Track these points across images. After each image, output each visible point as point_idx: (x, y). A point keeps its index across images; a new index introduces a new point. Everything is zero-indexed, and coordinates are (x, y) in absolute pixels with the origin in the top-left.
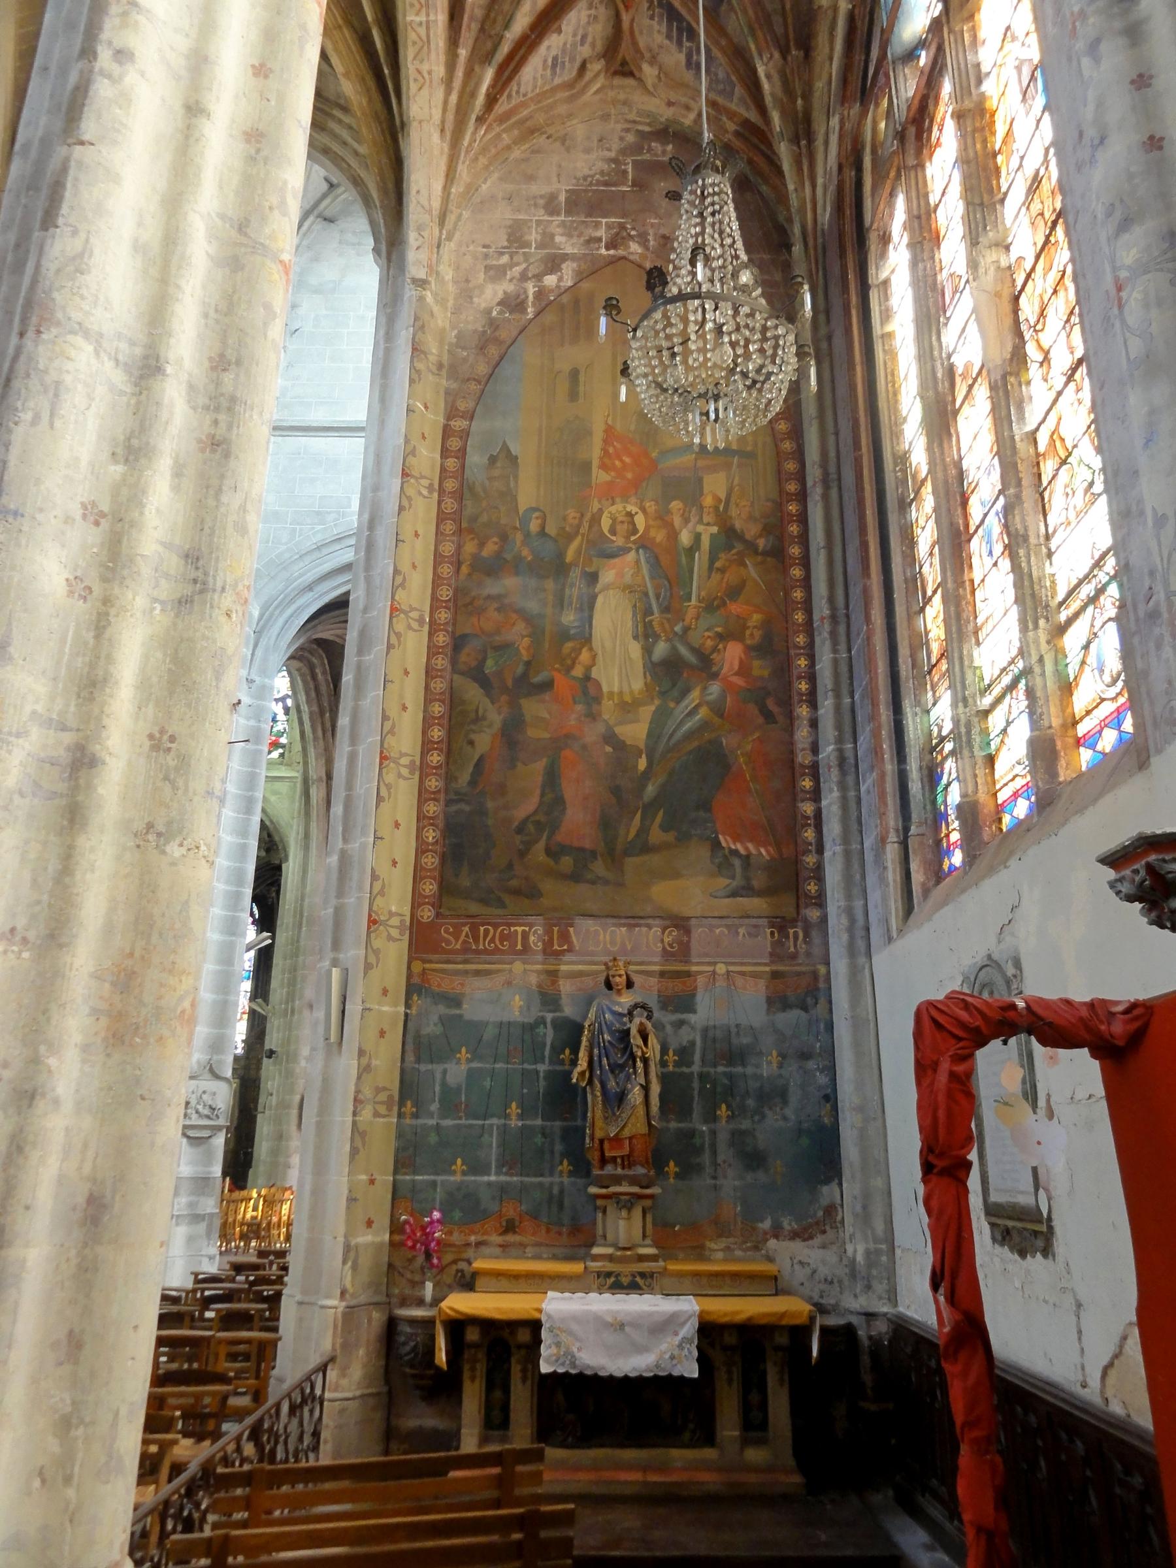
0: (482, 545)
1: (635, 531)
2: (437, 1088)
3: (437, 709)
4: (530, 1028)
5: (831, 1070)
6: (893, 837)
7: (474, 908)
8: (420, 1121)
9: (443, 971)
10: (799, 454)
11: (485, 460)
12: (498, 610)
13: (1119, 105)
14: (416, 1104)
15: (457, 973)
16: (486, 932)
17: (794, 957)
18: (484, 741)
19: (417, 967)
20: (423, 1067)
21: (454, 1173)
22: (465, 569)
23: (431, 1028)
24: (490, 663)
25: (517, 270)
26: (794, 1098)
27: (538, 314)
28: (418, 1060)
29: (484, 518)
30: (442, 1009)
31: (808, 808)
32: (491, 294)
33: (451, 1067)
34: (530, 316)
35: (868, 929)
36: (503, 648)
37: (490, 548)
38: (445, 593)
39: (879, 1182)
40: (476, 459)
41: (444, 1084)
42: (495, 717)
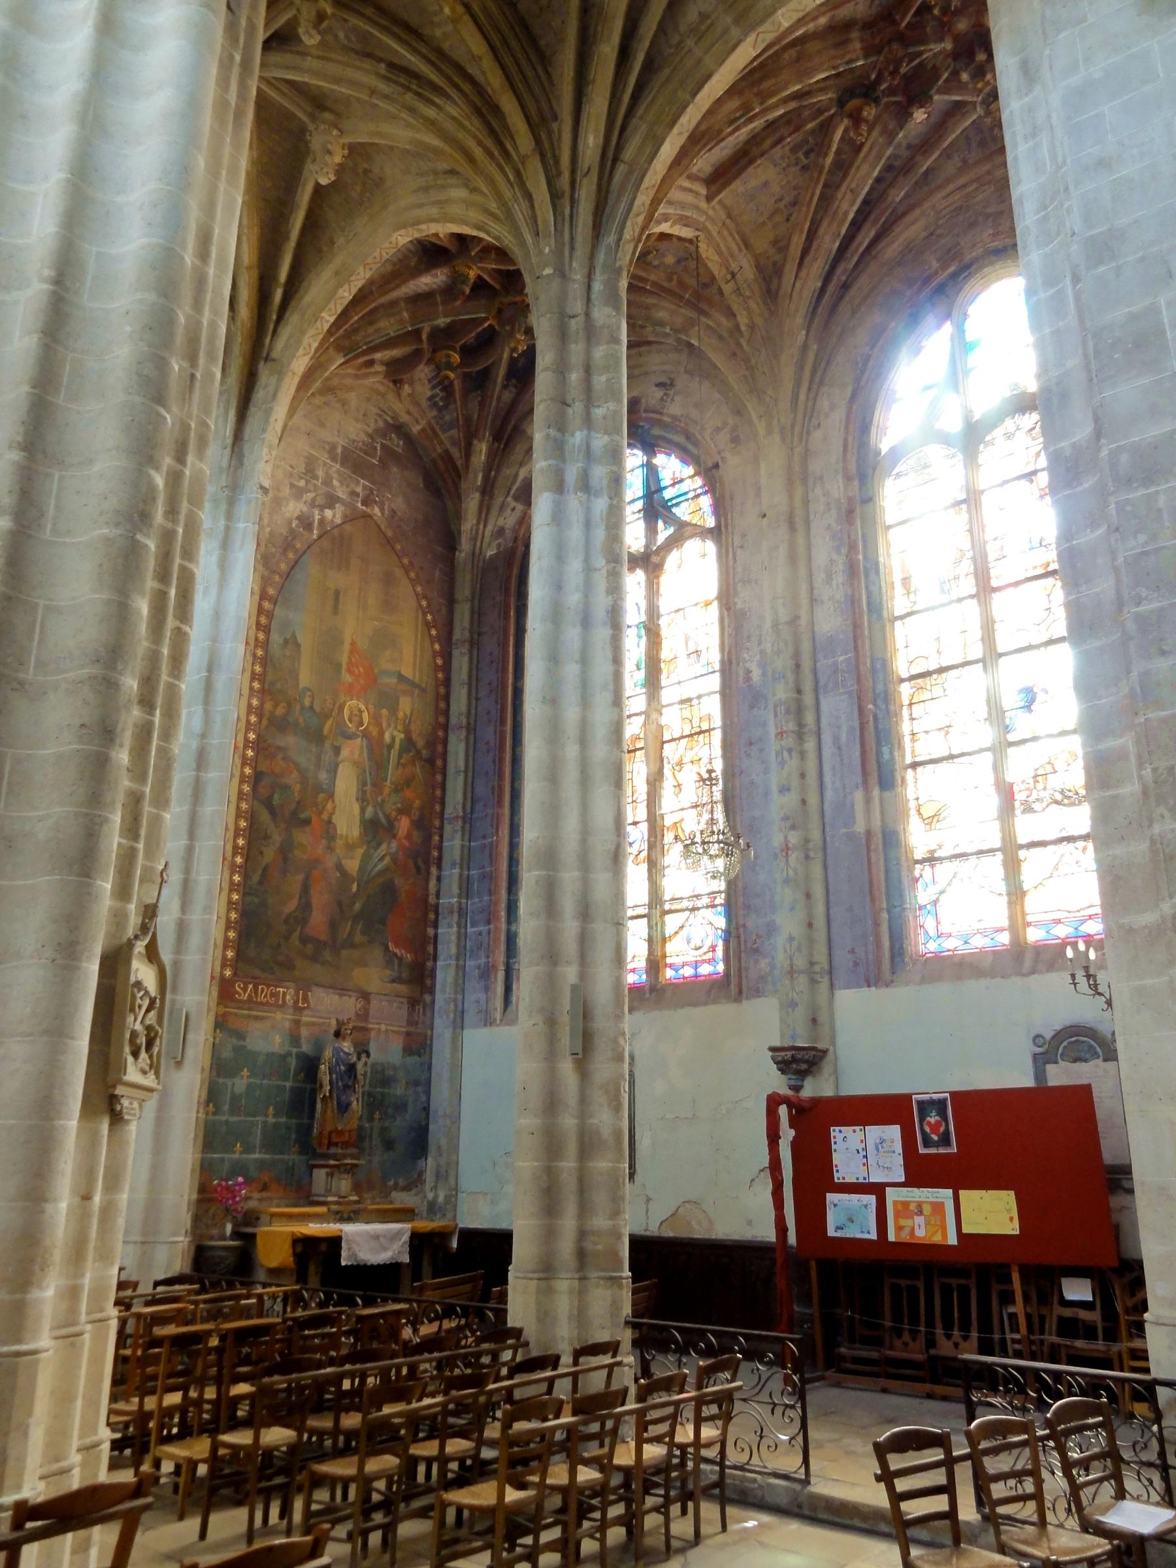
0: (276, 706)
1: (361, 724)
2: (229, 1096)
3: (243, 824)
4: (284, 1057)
5: (428, 1093)
6: (502, 967)
7: (257, 972)
8: (217, 1118)
9: (236, 1015)
10: (447, 698)
11: (281, 641)
12: (283, 759)
13: (795, 783)
14: (215, 1106)
15: (244, 1016)
16: (263, 990)
17: (417, 1023)
18: (270, 854)
19: (222, 1010)
20: (221, 1080)
21: (234, 1152)
22: (265, 722)
23: (227, 1054)
24: (276, 796)
25: (310, 496)
26: (410, 1109)
27: (320, 537)
28: (218, 1075)
29: (279, 686)
30: (234, 1041)
31: (431, 931)
32: (293, 508)
33: (237, 1081)
34: (315, 537)
35: (463, 1012)
36: (285, 787)
37: (280, 711)
38: (252, 736)
39: (454, 1158)
40: (275, 637)
41: (233, 1093)
42: (277, 838)
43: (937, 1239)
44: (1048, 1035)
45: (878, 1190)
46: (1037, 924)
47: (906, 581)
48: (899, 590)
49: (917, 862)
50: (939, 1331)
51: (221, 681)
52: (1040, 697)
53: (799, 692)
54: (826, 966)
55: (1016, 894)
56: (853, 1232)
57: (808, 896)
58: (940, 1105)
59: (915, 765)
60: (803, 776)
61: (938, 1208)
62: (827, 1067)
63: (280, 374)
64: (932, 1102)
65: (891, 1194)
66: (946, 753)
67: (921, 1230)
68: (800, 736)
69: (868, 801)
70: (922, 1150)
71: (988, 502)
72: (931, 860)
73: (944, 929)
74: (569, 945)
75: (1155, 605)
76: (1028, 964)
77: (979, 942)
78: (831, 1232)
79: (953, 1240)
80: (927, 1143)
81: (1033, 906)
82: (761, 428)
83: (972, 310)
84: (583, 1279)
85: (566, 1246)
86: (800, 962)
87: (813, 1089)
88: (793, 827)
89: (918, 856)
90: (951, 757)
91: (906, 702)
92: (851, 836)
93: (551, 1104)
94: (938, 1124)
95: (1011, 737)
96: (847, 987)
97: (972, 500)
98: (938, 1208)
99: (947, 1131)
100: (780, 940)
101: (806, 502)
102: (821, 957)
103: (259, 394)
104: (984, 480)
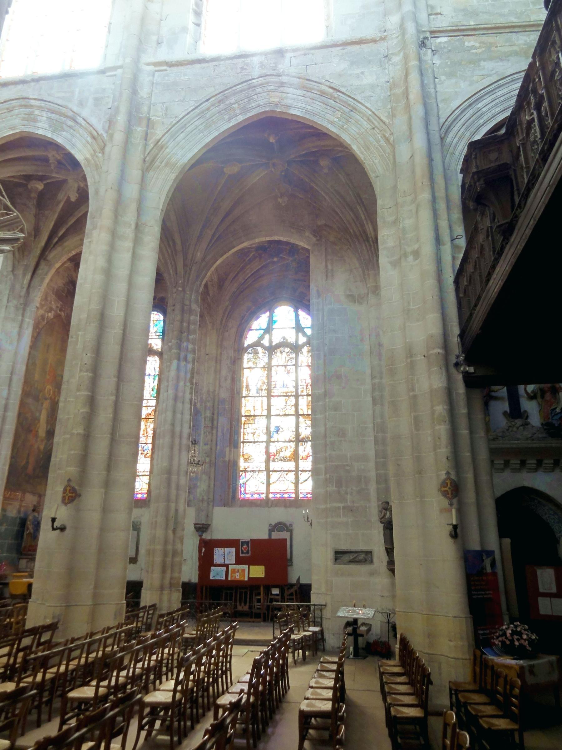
1: (50, 395)
4: (16, 518)
27: (46, 323)
32: (41, 312)
43: (242, 579)
44: (273, 524)
45: (227, 566)
46: (272, 493)
47: (247, 386)
48: (244, 388)
49: (241, 471)
50: (238, 604)
51: (15, 379)
52: (281, 430)
53: (213, 414)
54: (212, 500)
55: (268, 484)
56: (218, 578)
57: (209, 478)
58: (247, 543)
59: (243, 442)
60: (212, 441)
61: (244, 570)
62: (209, 530)
63: (50, 266)
64: (245, 542)
65: (231, 567)
66: (253, 441)
67: (238, 577)
68: (212, 428)
69: (230, 451)
70: (241, 555)
71: (273, 369)
72: (245, 471)
73: (247, 492)
74: (173, 497)
75: (333, 439)
76: (270, 504)
77: (256, 496)
78: (211, 578)
79: (246, 579)
80: (243, 553)
81: (272, 488)
82: (210, 326)
83: (275, 311)
84: (171, 590)
85: (167, 582)
86: (205, 498)
87: (207, 536)
88: (208, 456)
89: (241, 469)
90: (254, 442)
91: (243, 423)
92: (224, 461)
93: (166, 542)
94: (246, 548)
95: (272, 440)
96: (218, 506)
97: (268, 368)
98: (244, 570)
99: (248, 550)
100: (198, 490)
101: (221, 354)
102: (211, 496)
103: (39, 271)
104: (274, 362)
